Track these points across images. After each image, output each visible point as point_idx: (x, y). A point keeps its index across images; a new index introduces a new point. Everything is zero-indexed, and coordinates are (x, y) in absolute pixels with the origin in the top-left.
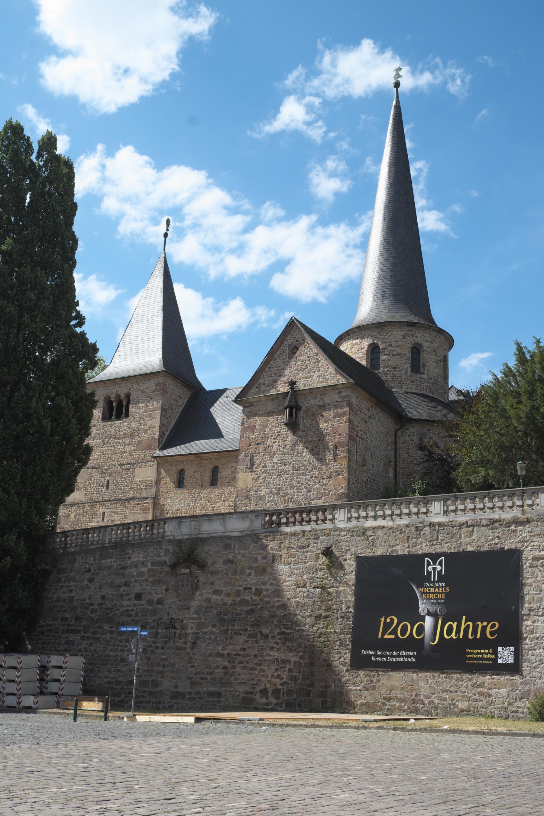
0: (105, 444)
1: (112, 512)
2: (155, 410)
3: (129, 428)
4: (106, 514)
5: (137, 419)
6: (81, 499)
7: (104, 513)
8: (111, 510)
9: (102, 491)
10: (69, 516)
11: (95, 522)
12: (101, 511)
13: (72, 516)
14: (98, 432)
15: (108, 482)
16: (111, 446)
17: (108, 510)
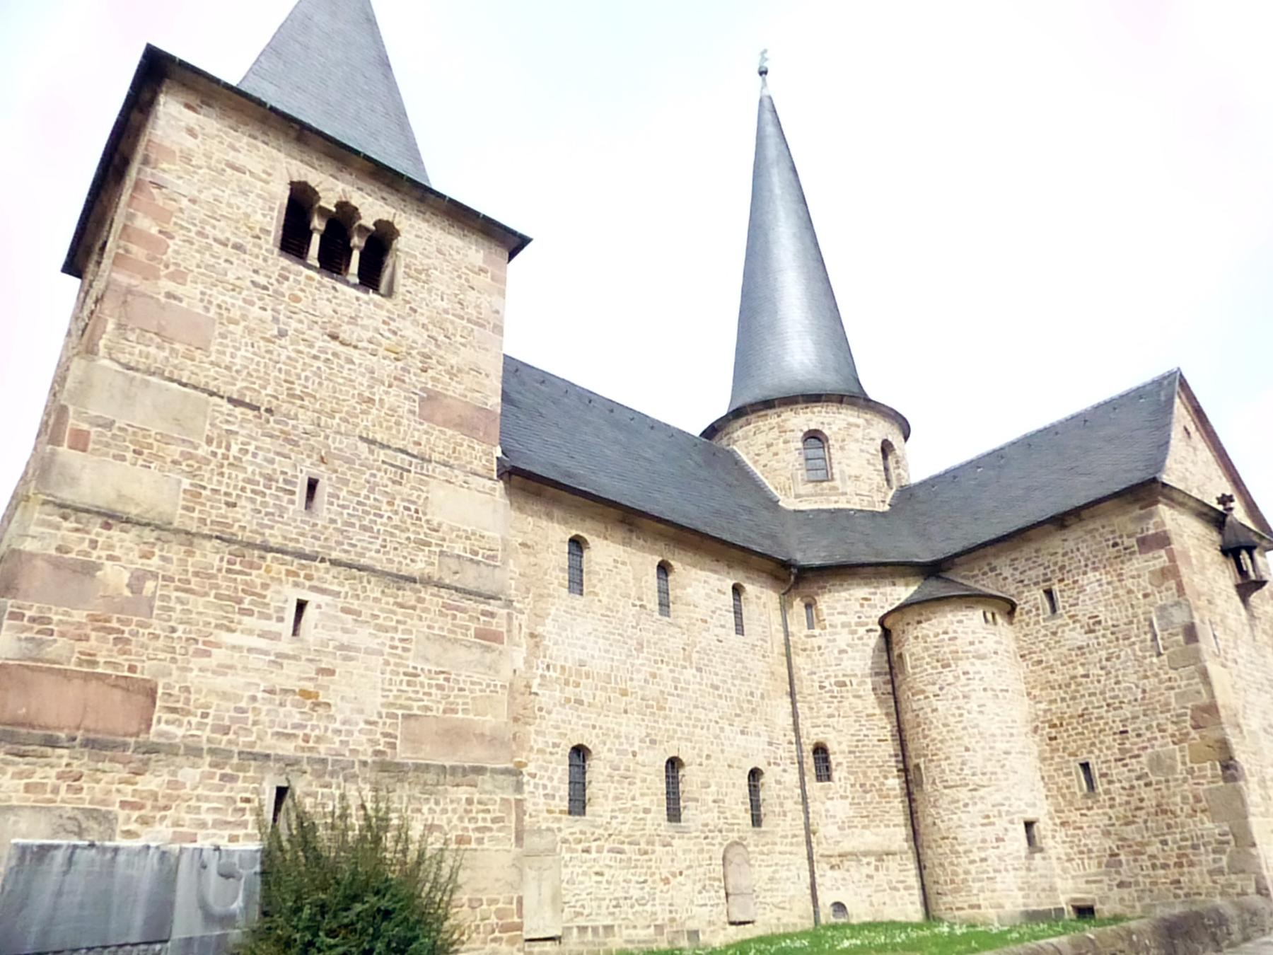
0: (282, 334)
1: (346, 611)
2: (483, 326)
3: (395, 333)
4: (309, 611)
5: (423, 320)
6: (166, 508)
7: (301, 606)
8: (340, 602)
9: (282, 510)
10: (88, 569)
11: (250, 632)
12: (295, 595)
13: (115, 576)
14: (262, 280)
15: (312, 485)
16: (315, 357)
17: (328, 599)
